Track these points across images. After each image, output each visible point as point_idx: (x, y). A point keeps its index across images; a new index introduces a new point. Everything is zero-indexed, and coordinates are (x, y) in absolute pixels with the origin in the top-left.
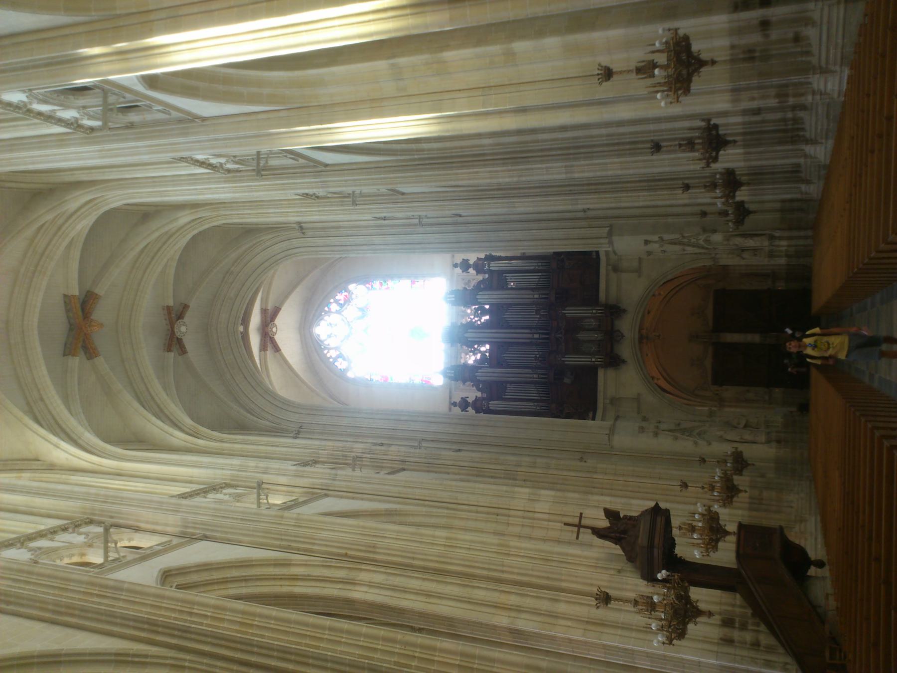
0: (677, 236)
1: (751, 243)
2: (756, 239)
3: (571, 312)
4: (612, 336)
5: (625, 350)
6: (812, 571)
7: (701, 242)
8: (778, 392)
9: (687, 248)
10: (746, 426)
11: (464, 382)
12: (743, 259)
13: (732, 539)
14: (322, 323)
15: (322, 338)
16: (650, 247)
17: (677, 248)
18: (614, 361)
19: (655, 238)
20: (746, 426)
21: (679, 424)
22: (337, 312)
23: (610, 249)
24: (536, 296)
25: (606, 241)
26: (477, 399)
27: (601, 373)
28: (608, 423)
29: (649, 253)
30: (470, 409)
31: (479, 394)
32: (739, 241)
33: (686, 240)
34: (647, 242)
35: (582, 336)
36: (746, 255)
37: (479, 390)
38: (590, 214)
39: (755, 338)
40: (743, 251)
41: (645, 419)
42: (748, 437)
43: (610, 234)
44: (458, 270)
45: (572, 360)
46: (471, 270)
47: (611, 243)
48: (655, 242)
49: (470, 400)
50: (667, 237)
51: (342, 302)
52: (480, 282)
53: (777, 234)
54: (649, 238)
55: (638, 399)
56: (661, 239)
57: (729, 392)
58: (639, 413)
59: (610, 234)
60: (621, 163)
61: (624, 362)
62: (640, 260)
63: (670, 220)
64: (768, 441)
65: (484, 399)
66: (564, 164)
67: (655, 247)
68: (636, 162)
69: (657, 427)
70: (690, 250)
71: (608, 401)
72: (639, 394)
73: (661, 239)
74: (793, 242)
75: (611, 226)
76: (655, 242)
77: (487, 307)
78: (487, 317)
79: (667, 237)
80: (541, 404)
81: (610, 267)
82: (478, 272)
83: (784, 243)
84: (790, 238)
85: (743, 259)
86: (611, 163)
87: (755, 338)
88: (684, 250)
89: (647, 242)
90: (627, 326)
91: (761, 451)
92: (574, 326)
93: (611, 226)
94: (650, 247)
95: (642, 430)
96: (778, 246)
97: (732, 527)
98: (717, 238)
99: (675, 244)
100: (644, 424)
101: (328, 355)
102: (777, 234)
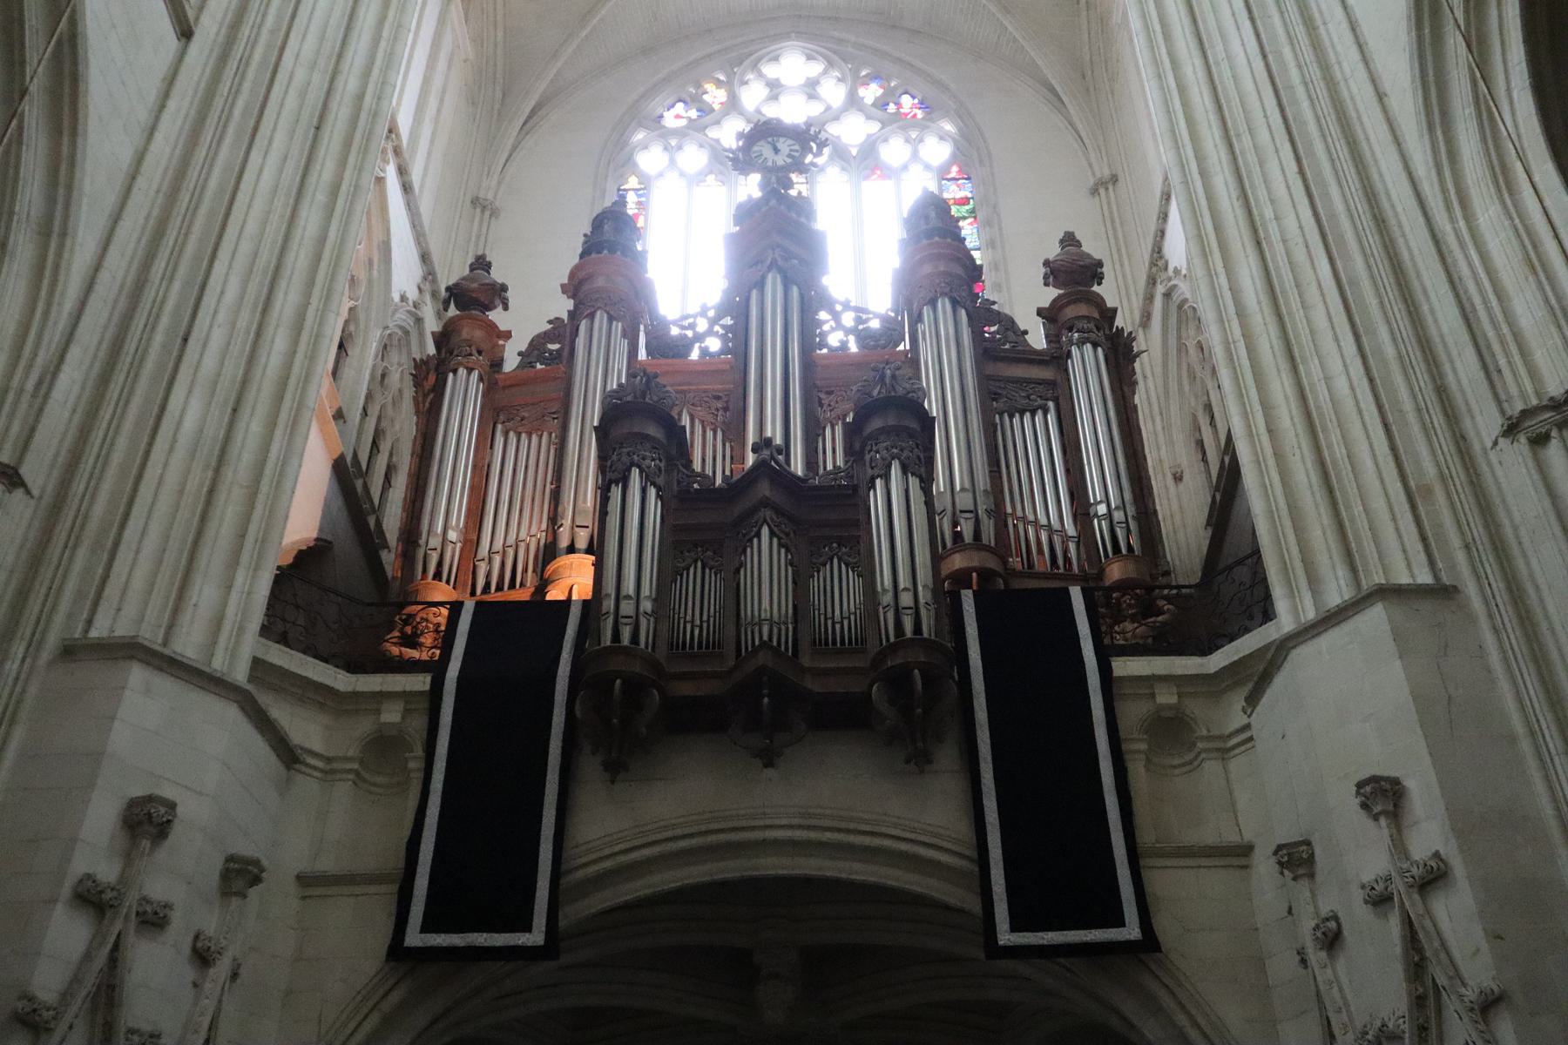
14: (816, 68)
15: (770, 70)
22: (853, 102)
29: (1297, 860)
37: (538, 344)
41: (241, 875)
47: (1331, 619)
50: (1455, 916)
51: (892, 108)
52: (1008, 324)
56: (1433, 878)
65: (497, 364)
73: (1433, 878)
75: (1443, 592)
81: (1166, 697)
89: (1383, 796)
95: (147, 822)
101: (709, 87)
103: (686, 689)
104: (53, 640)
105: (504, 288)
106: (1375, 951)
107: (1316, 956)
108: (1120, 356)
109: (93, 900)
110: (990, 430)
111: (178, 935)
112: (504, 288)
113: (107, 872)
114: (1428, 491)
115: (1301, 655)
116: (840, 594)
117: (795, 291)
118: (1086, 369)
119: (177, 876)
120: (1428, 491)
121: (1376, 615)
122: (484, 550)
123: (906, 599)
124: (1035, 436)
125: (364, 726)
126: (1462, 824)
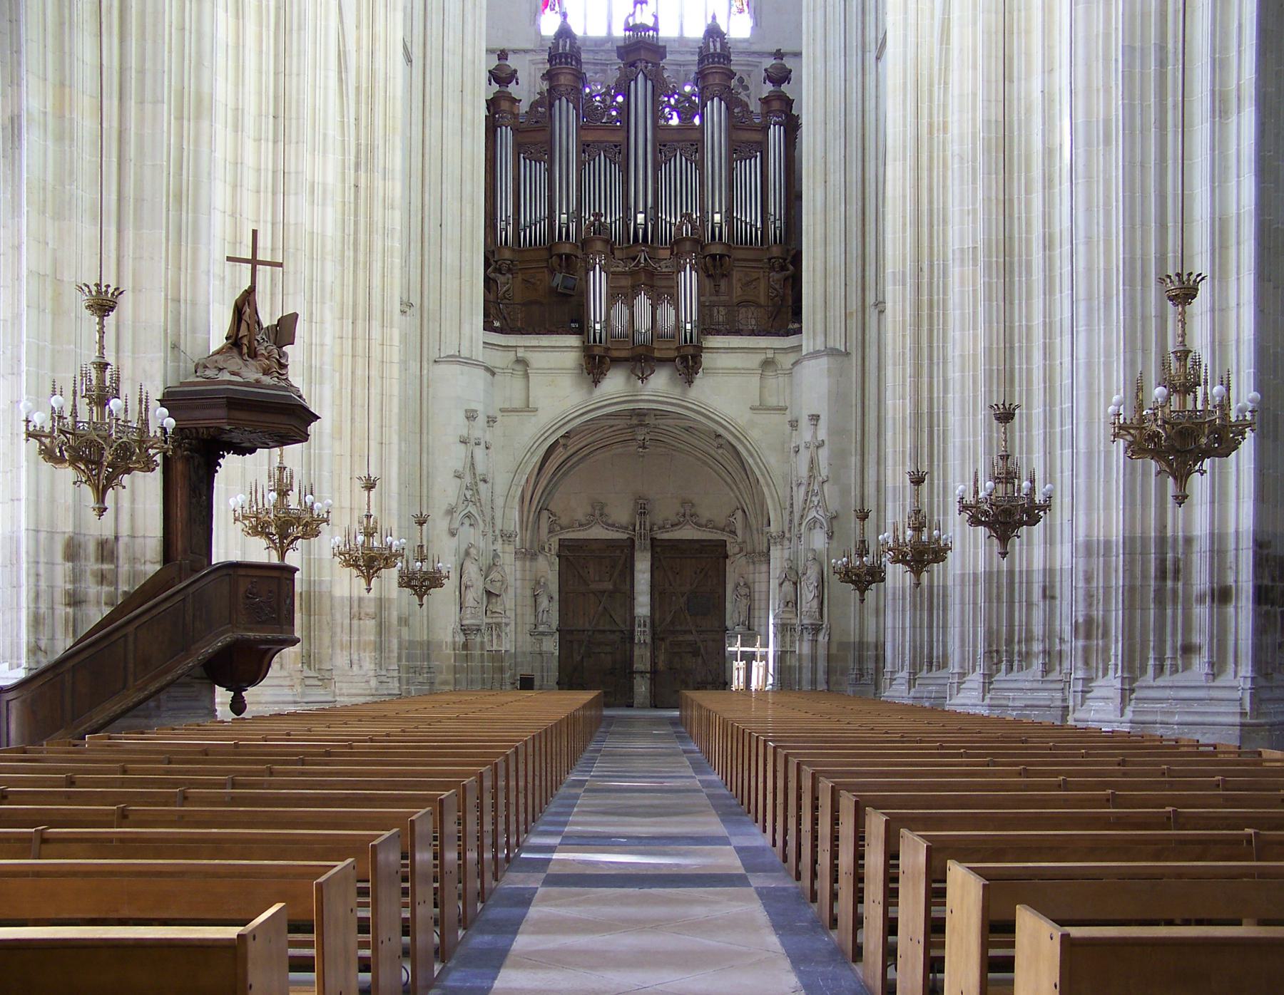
0: (824, 472)
1: (808, 595)
2: (815, 604)
3: (689, 281)
4: (640, 358)
5: (615, 384)
6: (222, 696)
7: (813, 514)
8: (551, 645)
9: (803, 489)
10: (489, 593)
11: (549, 76)
12: (781, 585)
13: (275, 559)
16: (804, 422)
17: (804, 471)
18: (595, 364)
19: (822, 434)
20: (489, 593)
21: (485, 481)
23: (804, 352)
24: (717, 217)
25: (820, 346)
26: (514, 101)
27: (573, 340)
28: (479, 353)
29: (794, 424)
30: (496, 87)
31: (524, 107)
32: (812, 574)
33: (816, 488)
34: (815, 418)
35: (643, 303)
36: (788, 587)
37: (534, 105)
38: (872, 315)
39: (643, 606)
40: (795, 584)
41: (491, 420)
42: (470, 596)
43: (832, 352)
44: (769, 62)
45: (598, 284)
46: (769, 87)
47: (815, 354)
48: (815, 433)
49: (512, 88)
52: (745, 106)
53: (823, 638)
54: (823, 423)
55: (528, 409)
57: (548, 569)
58: (502, 410)
59: (832, 352)
60: (975, 355)
61: (596, 382)
62: (783, 409)
63: (854, 460)
64: (465, 630)
65: (516, 116)
66: (980, 245)
67: (806, 434)
68: (975, 382)
69: (478, 444)
70: (800, 494)
71: (521, 353)
72: (536, 410)
74: (807, 664)
76: (815, 433)
77: (697, 121)
78: (675, 121)
79: (823, 454)
80: (510, 229)
81: (770, 355)
82: (766, 101)
83: (806, 649)
84: (814, 659)
85: (781, 585)
86: (975, 337)
87: (643, 606)
88: (799, 485)
90: (660, 384)
91: (443, 615)
92: (663, 290)
93: (847, 354)
94: (804, 422)
95: (471, 416)
96: (801, 640)
97: (292, 559)
98: (819, 540)
99: (811, 469)
100: (481, 419)
102: (823, 638)
103: (615, 354)
104: (431, 360)
105: (515, 71)
106: (804, 456)
107: (792, 453)
108: (792, 127)
109: (464, 442)
110: (731, 170)
111: (483, 445)
112: (515, 71)
113: (465, 433)
114: (851, 313)
115: (805, 363)
116: (667, 316)
117: (649, 83)
118: (775, 135)
119: (478, 429)
120: (851, 313)
121: (824, 362)
122: (522, 226)
123: (688, 326)
124: (749, 171)
125: (511, 355)
126: (831, 432)
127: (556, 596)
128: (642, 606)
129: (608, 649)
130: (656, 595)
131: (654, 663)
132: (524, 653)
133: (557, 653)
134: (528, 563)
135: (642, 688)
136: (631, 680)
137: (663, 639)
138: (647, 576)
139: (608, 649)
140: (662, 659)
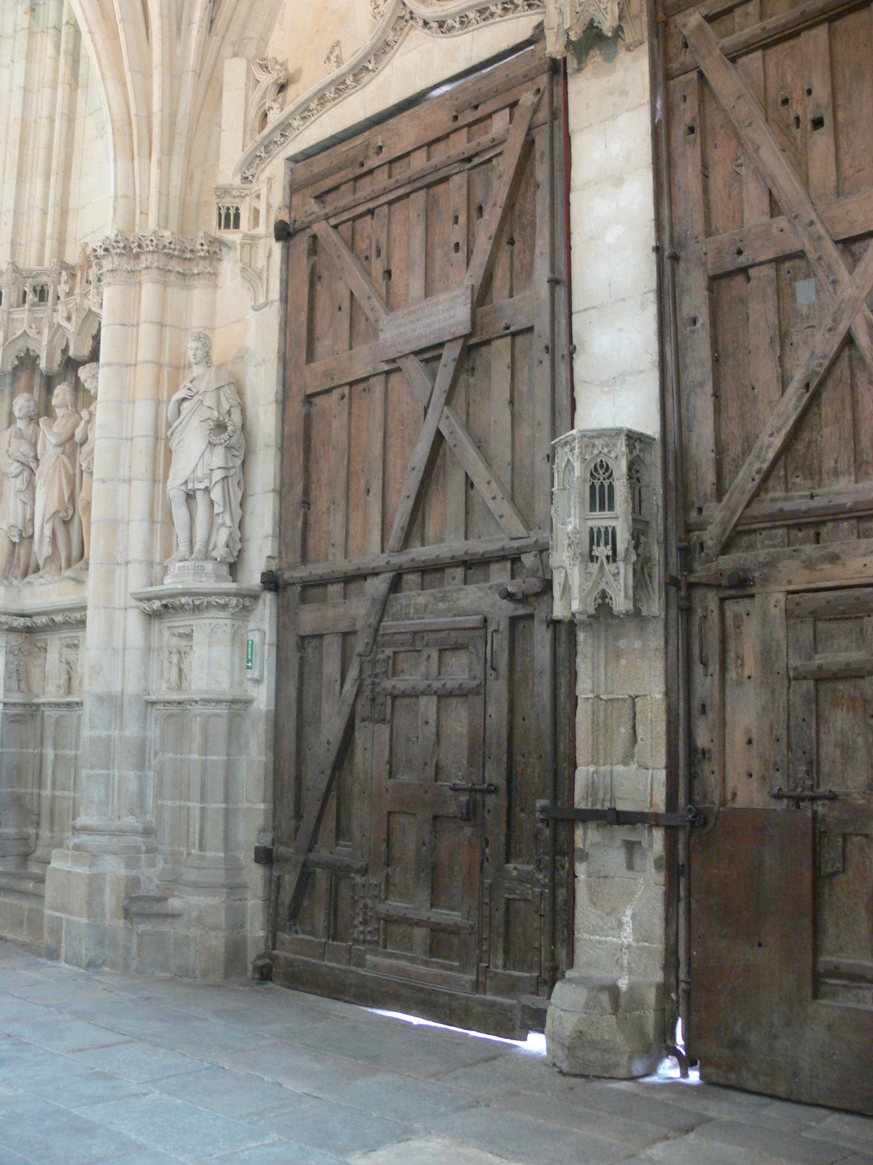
8: (230, 664)
39: (618, 381)
87: (618, 381)
127: (266, 422)
128: (617, 381)
129: (459, 670)
130: (695, 300)
131: (686, 760)
132: (112, 703)
133: (262, 697)
134: (149, 291)
135: (621, 920)
136: (560, 858)
137: (741, 585)
138: (637, 194)
139: (459, 670)
140: (747, 714)
